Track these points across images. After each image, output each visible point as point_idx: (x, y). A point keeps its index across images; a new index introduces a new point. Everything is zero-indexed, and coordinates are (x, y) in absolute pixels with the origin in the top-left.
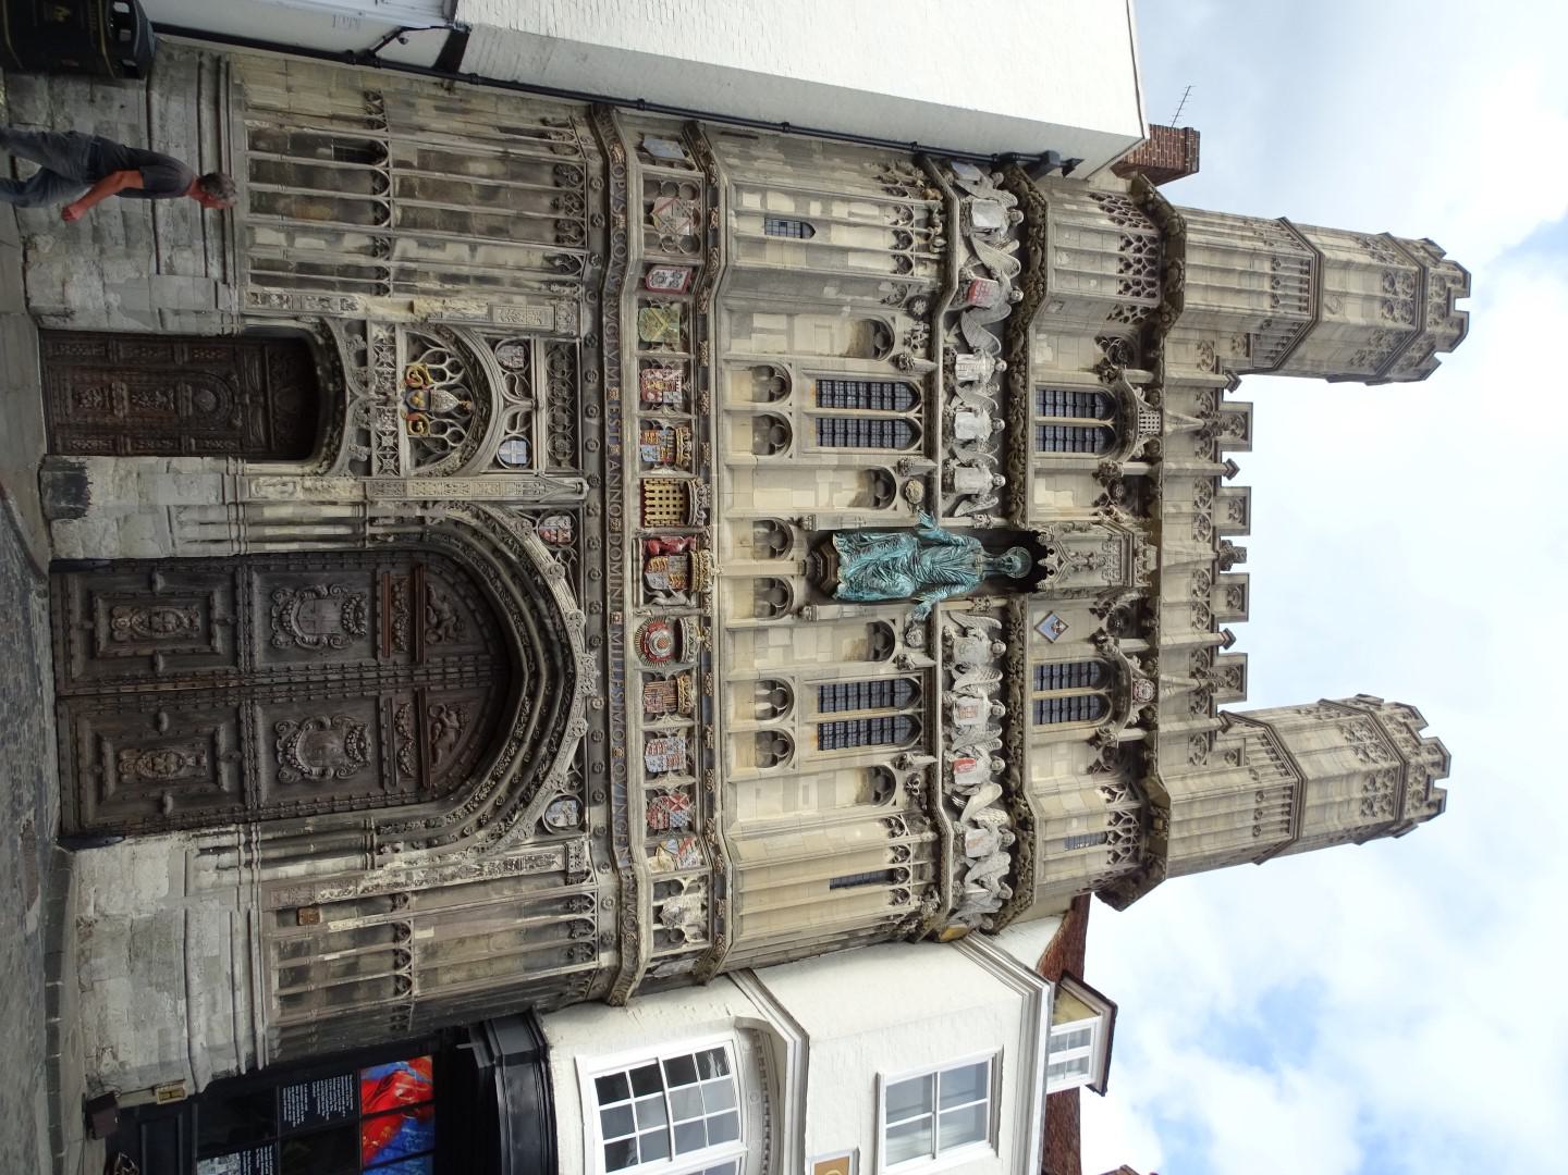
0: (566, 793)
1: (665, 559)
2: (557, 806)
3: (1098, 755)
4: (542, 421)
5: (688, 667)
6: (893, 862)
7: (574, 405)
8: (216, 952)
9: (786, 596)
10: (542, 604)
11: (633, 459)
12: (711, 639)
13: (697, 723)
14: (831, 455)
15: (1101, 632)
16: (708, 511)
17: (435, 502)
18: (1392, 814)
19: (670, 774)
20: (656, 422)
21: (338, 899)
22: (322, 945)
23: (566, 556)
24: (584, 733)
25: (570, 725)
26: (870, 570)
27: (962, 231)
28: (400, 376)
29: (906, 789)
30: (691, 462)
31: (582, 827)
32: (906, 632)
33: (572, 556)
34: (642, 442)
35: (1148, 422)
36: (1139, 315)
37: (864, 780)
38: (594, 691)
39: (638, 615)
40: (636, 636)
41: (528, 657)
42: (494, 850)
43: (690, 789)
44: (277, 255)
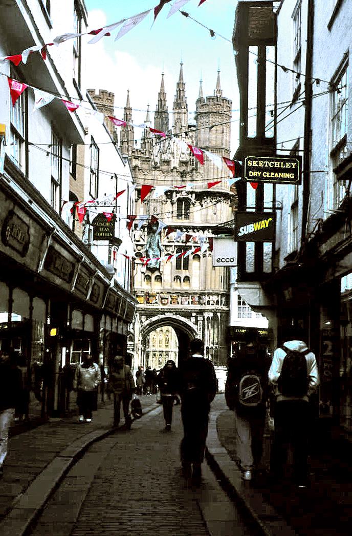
9: (158, 276)
15: (171, 202)
43: (192, 296)
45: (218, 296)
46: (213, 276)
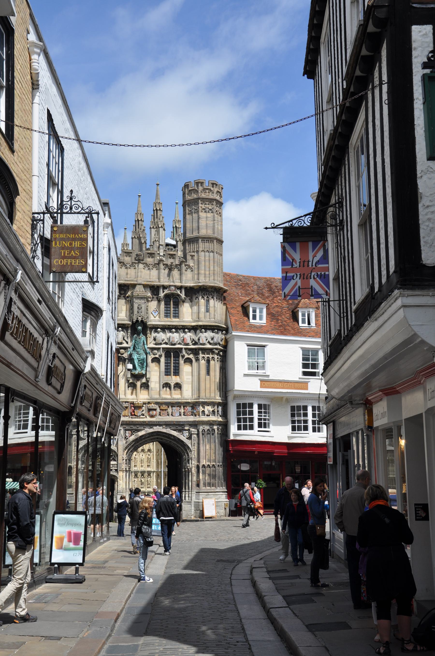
3: (188, 298)
9: (144, 383)
10: (143, 437)
15: (157, 298)
16: (126, 402)
23: (134, 432)
25: (168, 432)
29: (189, 355)
31: (189, 430)
32: (154, 354)
33: (133, 431)
38: (162, 427)
39: (146, 417)
42: (191, 448)
43: (184, 407)
45: (214, 406)
46: (208, 382)
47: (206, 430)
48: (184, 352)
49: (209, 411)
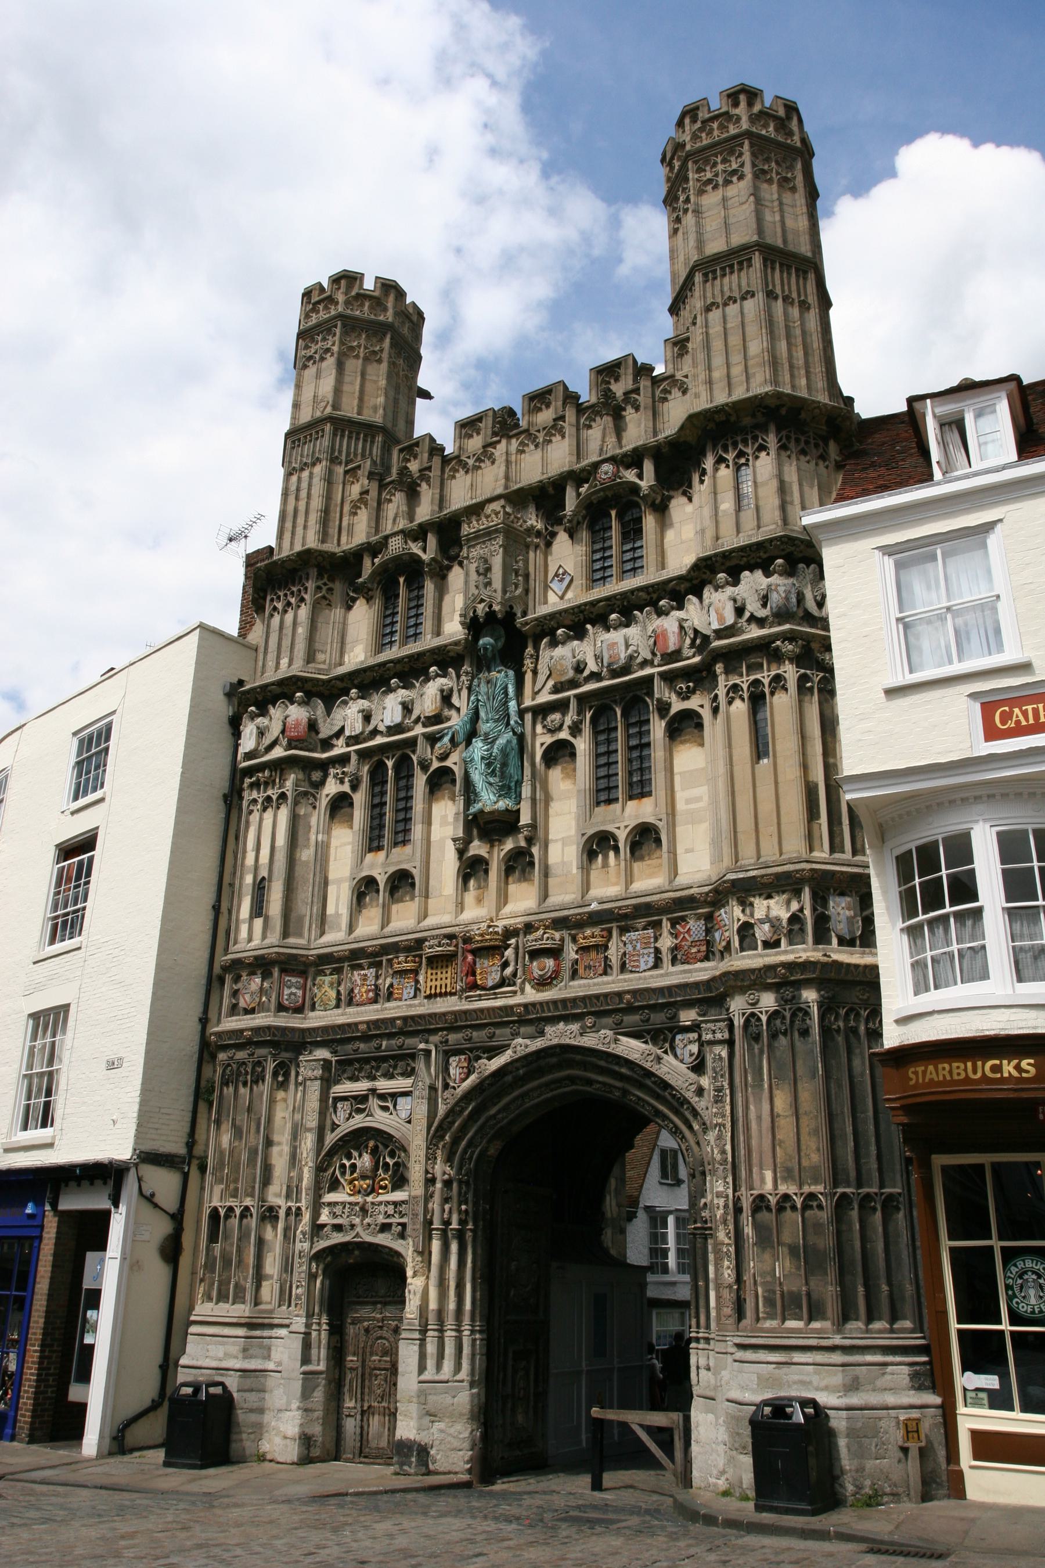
0: (667, 1045)
1: (478, 971)
2: (679, 1052)
4: (384, 1085)
5: (568, 939)
6: (743, 700)
7: (375, 1059)
8: (754, 1377)
10: (509, 1078)
11: (410, 1006)
12: (541, 920)
13: (614, 925)
14: (417, 830)
17: (427, 1172)
18: (741, 145)
19: (657, 945)
20: (388, 989)
21: (734, 1262)
22: (769, 1279)
24: (609, 1033)
25: (601, 1047)
26: (491, 780)
27: (262, 756)
28: (352, 1199)
29: (688, 698)
30: (414, 956)
32: (551, 732)
34: (400, 999)
35: (396, 545)
36: (325, 580)
37: (682, 742)
38: (575, 1027)
39: (522, 990)
40: (538, 991)
41: (560, 1087)
43: (674, 923)
44: (277, 1287)
45: (797, 893)
46: (765, 793)
47: (764, 1018)
48: (661, 691)
49: (774, 923)
